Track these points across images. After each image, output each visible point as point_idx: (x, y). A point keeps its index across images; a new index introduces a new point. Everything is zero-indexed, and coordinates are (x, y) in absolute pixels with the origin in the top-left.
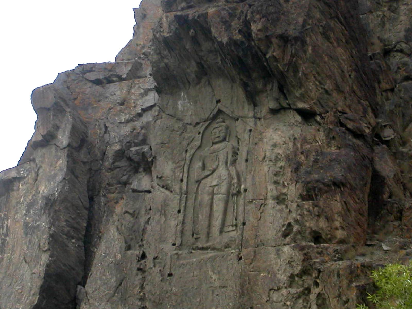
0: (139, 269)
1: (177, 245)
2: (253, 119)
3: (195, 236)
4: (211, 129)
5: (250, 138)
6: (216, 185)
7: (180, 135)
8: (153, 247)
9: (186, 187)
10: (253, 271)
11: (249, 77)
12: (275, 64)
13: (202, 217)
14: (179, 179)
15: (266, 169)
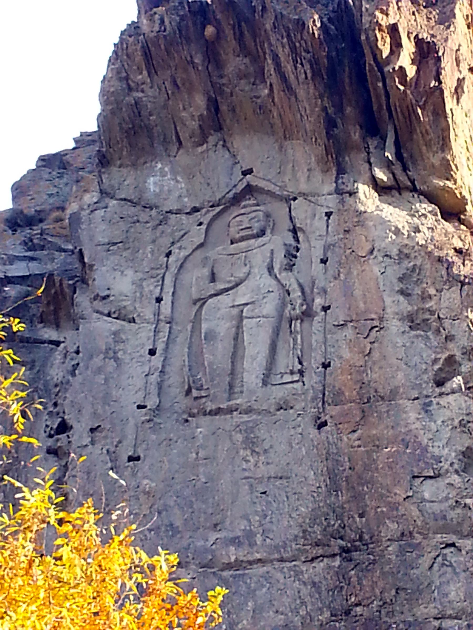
0: (52, 452)
1: (148, 407)
2: (335, 196)
3: (195, 393)
4: (227, 217)
5: (328, 226)
6: (247, 304)
7: (155, 228)
8: (87, 411)
9: (169, 310)
10: (359, 446)
11: (340, 108)
15: (376, 270)
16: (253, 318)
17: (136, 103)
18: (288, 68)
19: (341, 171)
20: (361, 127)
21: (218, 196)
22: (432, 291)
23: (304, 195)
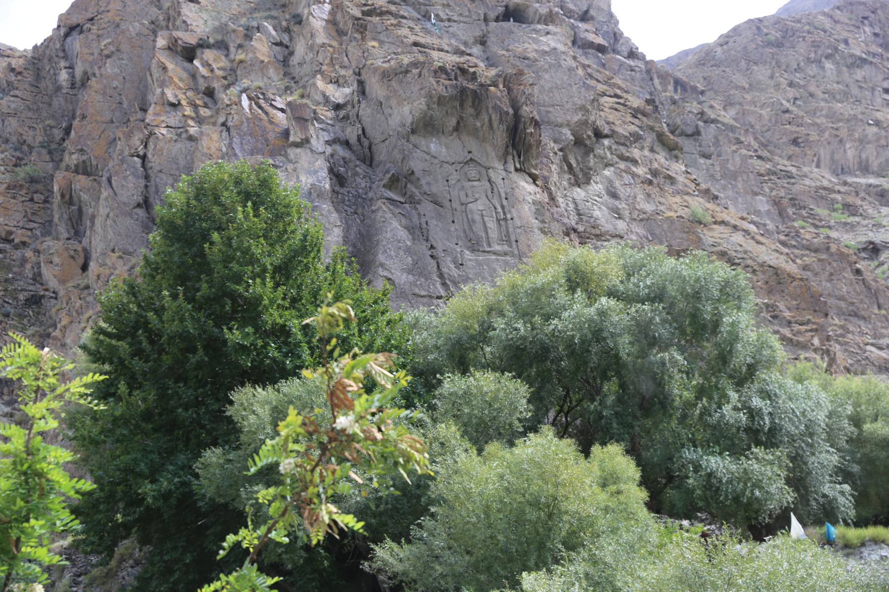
19: (506, 162)
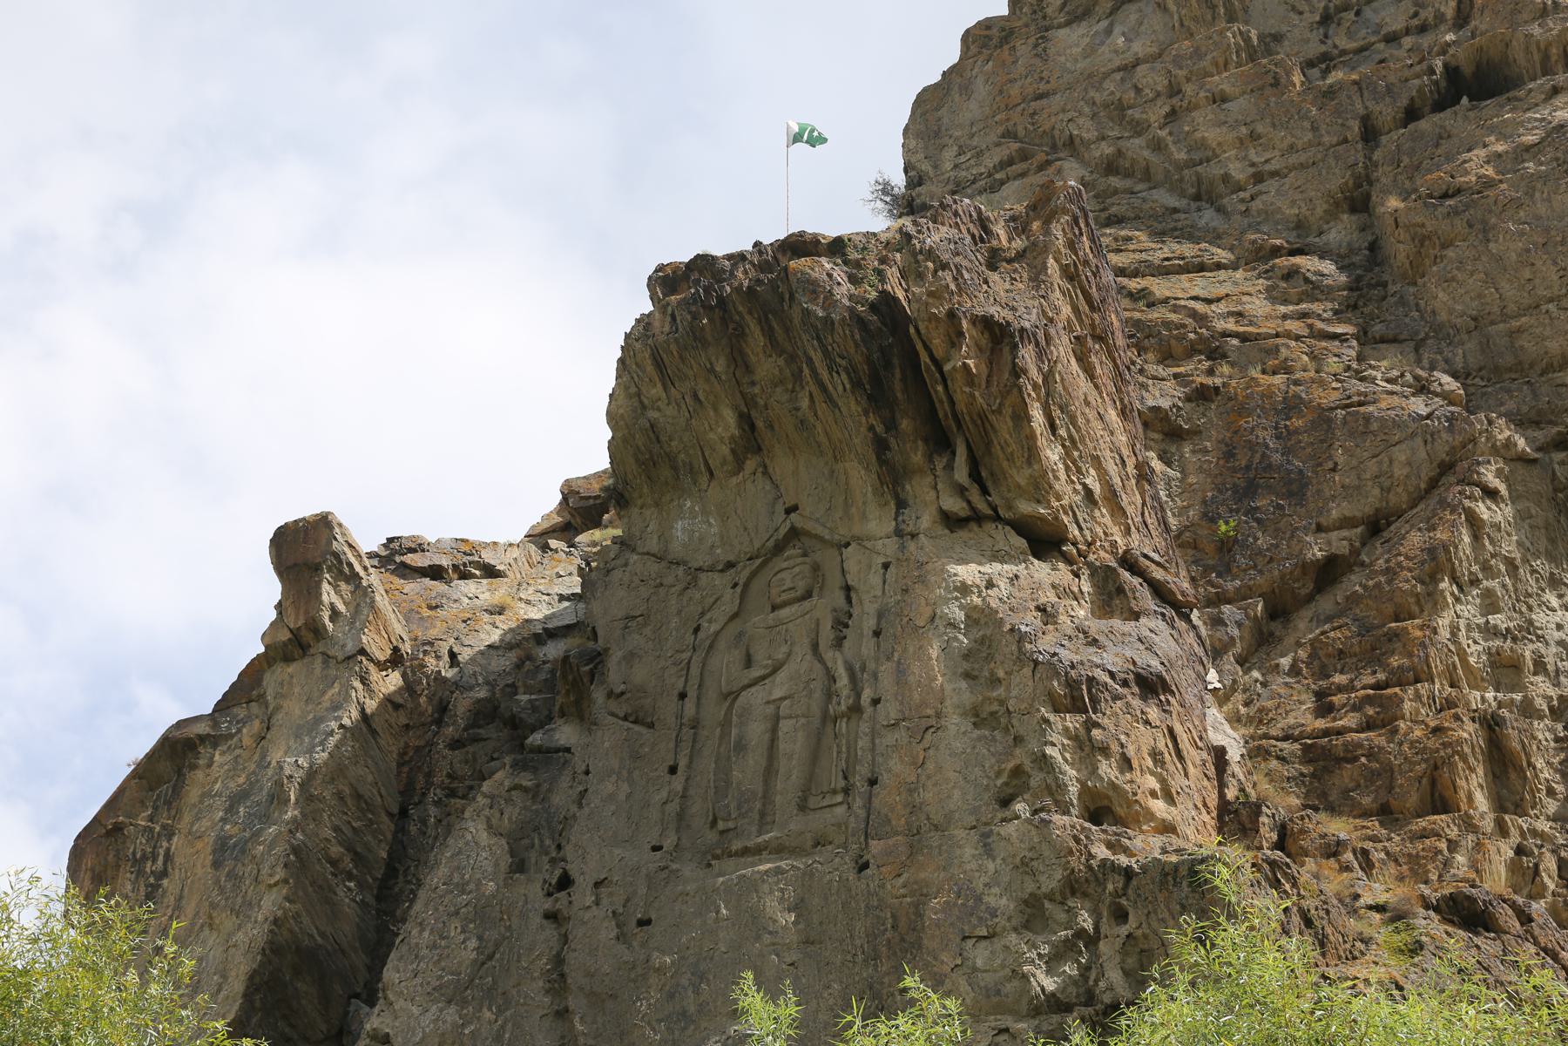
0: (552, 916)
3: (721, 825)
11: (891, 425)
12: (967, 389)
13: (747, 772)
14: (676, 692)
16: (790, 717)
17: (652, 426)
18: (824, 375)
19: (901, 504)
20: (926, 440)
21: (757, 545)
22: (1001, 674)
23: (859, 539)
